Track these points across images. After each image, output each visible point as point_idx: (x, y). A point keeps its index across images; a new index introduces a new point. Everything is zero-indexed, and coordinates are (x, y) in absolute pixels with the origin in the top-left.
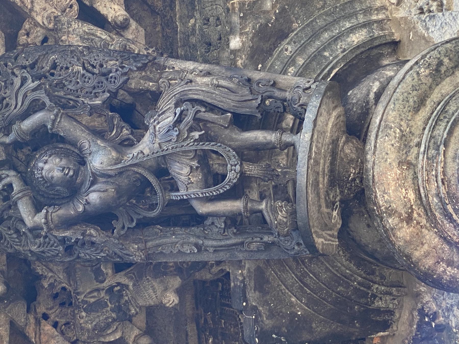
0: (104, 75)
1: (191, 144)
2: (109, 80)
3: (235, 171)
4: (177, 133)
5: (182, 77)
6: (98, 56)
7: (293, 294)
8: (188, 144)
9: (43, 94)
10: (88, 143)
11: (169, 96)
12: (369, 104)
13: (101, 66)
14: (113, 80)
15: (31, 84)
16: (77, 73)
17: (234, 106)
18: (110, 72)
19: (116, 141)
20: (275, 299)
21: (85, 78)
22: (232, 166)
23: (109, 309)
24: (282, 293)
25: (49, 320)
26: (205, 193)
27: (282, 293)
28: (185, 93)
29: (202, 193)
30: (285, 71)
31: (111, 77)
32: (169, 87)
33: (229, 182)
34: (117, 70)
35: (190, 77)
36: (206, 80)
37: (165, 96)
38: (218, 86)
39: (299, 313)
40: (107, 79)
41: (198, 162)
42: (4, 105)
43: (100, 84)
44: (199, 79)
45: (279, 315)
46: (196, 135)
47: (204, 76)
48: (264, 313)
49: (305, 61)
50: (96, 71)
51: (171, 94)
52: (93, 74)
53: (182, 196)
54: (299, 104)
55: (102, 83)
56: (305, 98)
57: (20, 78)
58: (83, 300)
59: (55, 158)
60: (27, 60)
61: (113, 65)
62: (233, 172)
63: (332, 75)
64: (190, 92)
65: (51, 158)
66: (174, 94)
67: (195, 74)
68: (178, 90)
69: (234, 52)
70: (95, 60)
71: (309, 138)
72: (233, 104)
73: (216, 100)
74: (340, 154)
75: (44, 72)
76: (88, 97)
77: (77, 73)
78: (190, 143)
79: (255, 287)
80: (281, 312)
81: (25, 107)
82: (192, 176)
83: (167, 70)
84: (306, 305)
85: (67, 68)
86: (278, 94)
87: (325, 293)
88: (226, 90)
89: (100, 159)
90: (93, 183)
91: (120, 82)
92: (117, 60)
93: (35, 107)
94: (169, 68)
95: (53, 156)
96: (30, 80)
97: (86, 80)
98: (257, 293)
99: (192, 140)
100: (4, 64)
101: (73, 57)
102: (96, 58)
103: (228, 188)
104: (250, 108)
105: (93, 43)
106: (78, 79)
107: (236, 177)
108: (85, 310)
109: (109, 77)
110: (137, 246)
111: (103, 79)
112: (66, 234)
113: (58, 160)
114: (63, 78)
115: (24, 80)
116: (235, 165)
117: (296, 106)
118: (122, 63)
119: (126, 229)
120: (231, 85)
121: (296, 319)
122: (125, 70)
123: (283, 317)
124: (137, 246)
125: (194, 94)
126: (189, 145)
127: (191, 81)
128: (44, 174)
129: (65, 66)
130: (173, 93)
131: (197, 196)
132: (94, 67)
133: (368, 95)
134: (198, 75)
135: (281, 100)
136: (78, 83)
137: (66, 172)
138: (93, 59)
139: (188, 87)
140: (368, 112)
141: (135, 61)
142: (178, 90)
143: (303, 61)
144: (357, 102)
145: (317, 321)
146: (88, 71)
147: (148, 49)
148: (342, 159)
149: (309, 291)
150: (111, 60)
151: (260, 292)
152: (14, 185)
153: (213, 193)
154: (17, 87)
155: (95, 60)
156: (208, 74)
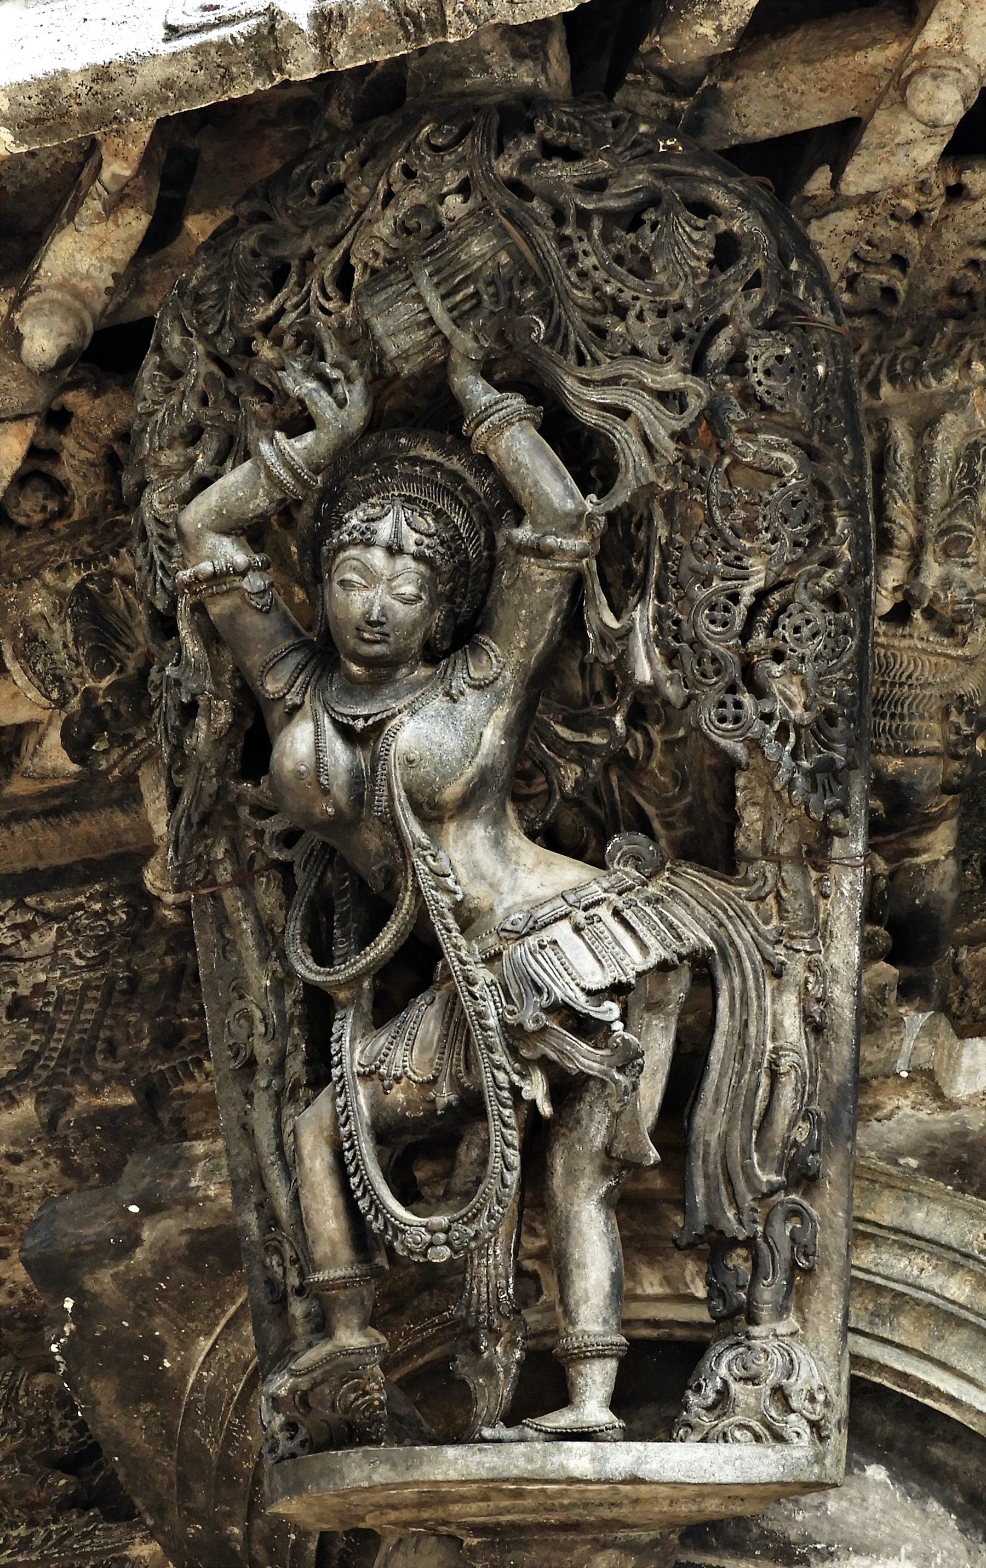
0: (748, 670)
1: (501, 1076)
2: (729, 699)
3: (431, 1244)
4: (530, 1026)
5: (792, 938)
6: (814, 636)
7: (215, 1343)
8: (499, 1067)
9: (638, 479)
10: (491, 674)
11: (720, 906)
12: (824, 1560)
13: (778, 656)
14: (730, 711)
15: (662, 426)
16: (741, 572)
17: (707, 1144)
18: (760, 692)
19: (538, 745)
20: (184, 1291)
21: (726, 609)
22: (447, 1231)
23: (90, 683)
24: (211, 1310)
25: (53, 432)
26: (352, 1146)
27: (211, 1310)
28: (734, 963)
29: (350, 1136)
30: (912, 1248)
31: (738, 705)
32: (749, 899)
33: (396, 1229)
34: (767, 718)
35: (797, 969)
36: (792, 1025)
37: (719, 892)
38: (774, 1076)
39: (167, 1364)
40: (732, 689)
41: (449, 1106)
42: (597, 321)
43: (709, 668)
44: (790, 1000)
45: (139, 1307)
46: (536, 1089)
47: (806, 1017)
48: (127, 1267)
49: (962, 1306)
50: (760, 637)
51: (725, 911)
52: (745, 635)
53: (340, 1062)
54: (731, 1380)
55: (717, 672)
56: (752, 1401)
57: (681, 384)
58: (110, 574)
59: (414, 576)
60: (767, 373)
61: (788, 699)
62: (428, 1237)
63: (928, 1402)
64: (737, 981)
65: (412, 564)
66: (726, 922)
67: (806, 982)
68: (740, 935)
69: (929, 1081)
70: (797, 630)
71: (577, 1474)
72: (714, 1143)
73: (722, 1076)
74: (585, 1542)
75: (732, 446)
76: (661, 629)
77: (741, 572)
78: (507, 1073)
79: (200, 1232)
80: (151, 1314)
81: (590, 417)
82: (409, 1086)
83: (814, 875)
84: (199, 1379)
85: (751, 530)
86: (767, 1293)
87: (245, 1439)
88: (760, 1105)
89: (445, 728)
90: (346, 733)
91: (723, 742)
92: (806, 708)
93: (586, 456)
94: (820, 881)
95: (422, 568)
96: (678, 426)
97: (718, 615)
98: (184, 1239)
99: (515, 1078)
100: (757, 274)
101: (797, 544)
102: (806, 631)
103: (374, 1225)
104: (712, 1203)
105: (961, 495)
106: (723, 579)
107: (411, 1252)
108: (80, 587)
109: (738, 696)
110: (220, 856)
111: (734, 672)
112: (188, 641)
113: (409, 589)
114: (715, 525)
115: (671, 399)
116: (448, 1243)
117: (723, 1371)
118: (798, 727)
119: (260, 824)
120: (781, 1121)
121: (146, 1358)
122: (771, 749)
123: (136, 1321)
124: (219, 853)
125: (732, 998)
126: (497, 1071)
127: (778, 975)
128: (353, 552)
129: (761, 524)
130: (729, 917)
131: (342, 1119)
132: (772, 627)
133: (857, 1552)
134: (804, 995)
135: (749, 1302)
136: (706, 583)
137: (366, 635)
138: (798, 620)
139: (755, 971)
140: (798, 1562)
141: (810, 775)
142: (740, 935)
143: (962, 1300)
144: (828, 1518)
145: (164, 1417)
146: (754, 610)
147: (960, 711)
148: (569, 1549)
149: (238, 1388)
150: (804, 685)
151: (189, 1246)
152: (309, 437)
153: (354, 1174)
154: (648, 380)
155: (797, 630)
156: (816, 1028)
